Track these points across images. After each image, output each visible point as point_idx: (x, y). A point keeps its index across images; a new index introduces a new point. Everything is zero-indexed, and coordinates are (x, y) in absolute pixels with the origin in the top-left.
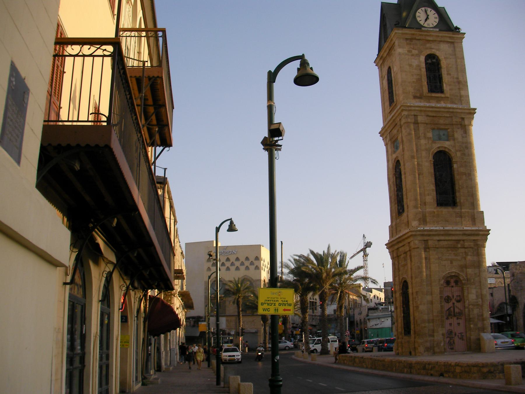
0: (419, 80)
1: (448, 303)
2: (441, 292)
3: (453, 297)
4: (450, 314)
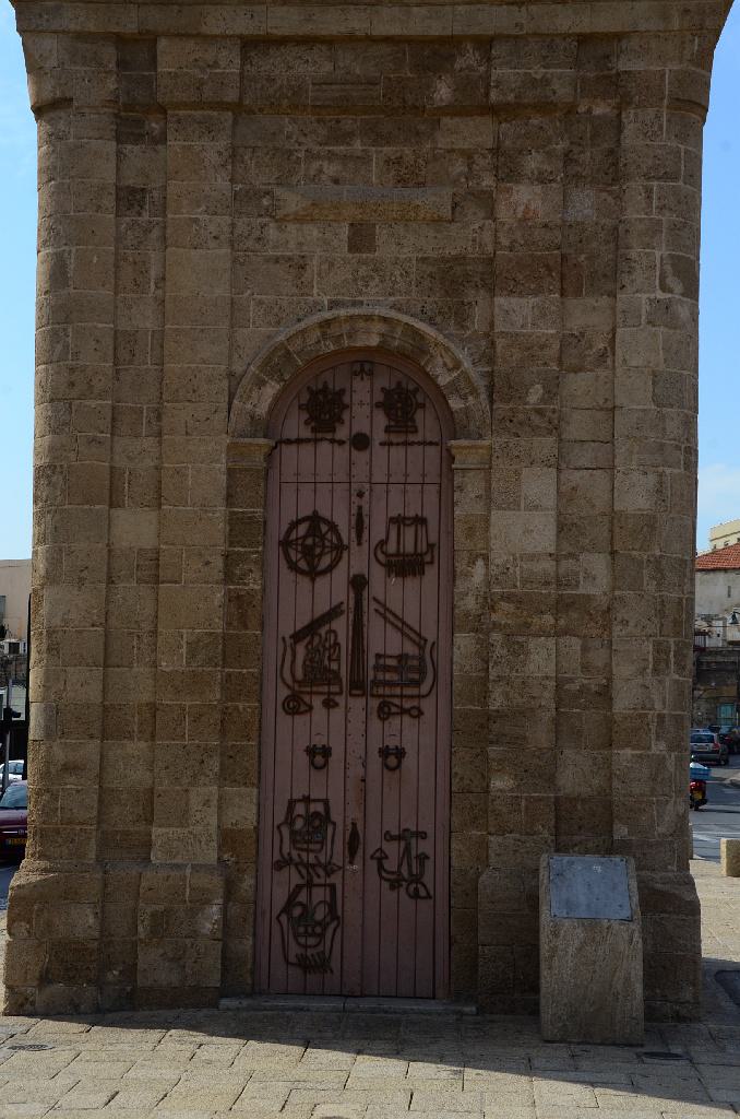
1: (313, 574)
2: (249, 481)
3: (360, 527)
4: (325, 668)
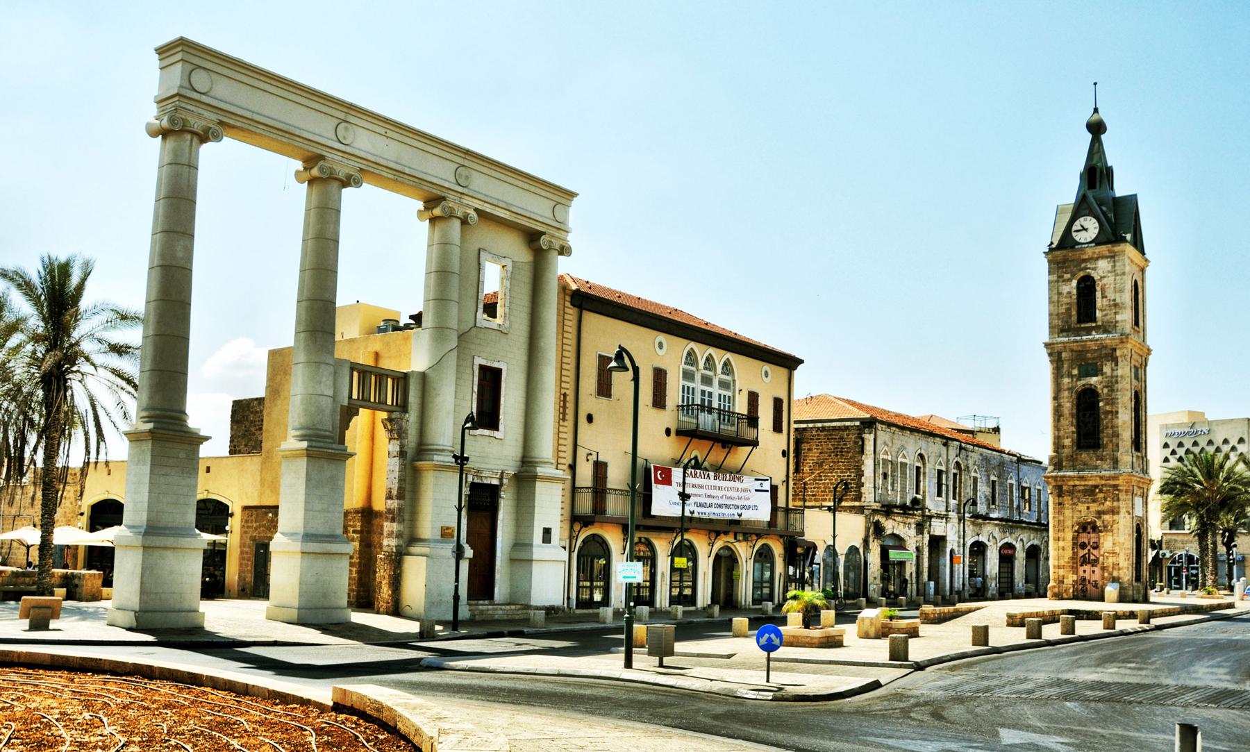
0: (1068, 310)
4: (1085, 561)
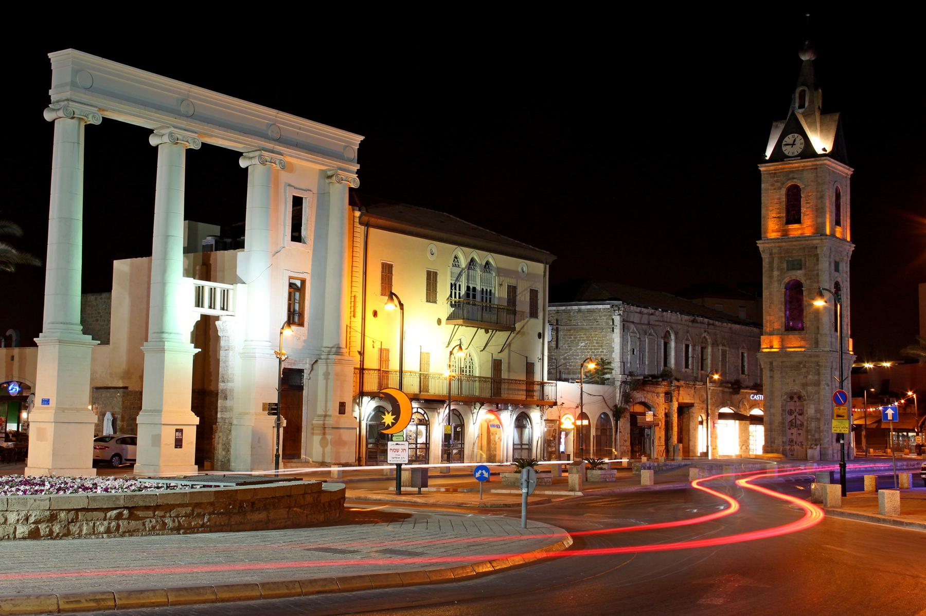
4: (792, 424)
